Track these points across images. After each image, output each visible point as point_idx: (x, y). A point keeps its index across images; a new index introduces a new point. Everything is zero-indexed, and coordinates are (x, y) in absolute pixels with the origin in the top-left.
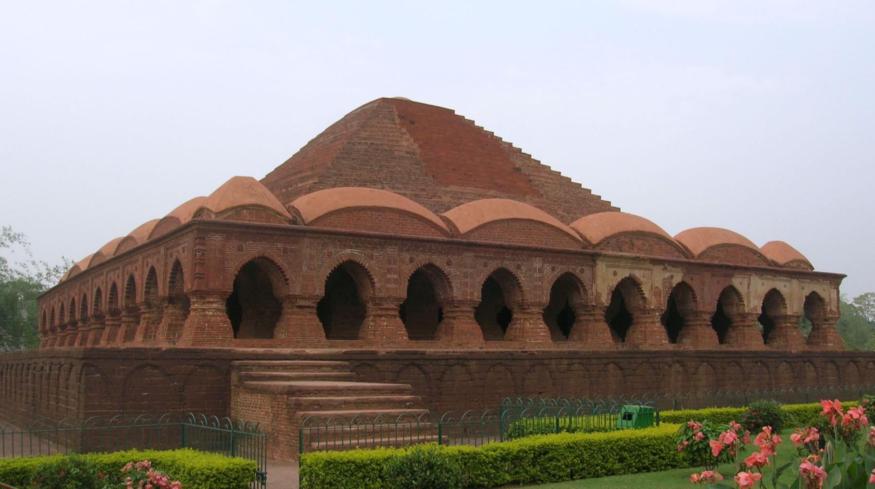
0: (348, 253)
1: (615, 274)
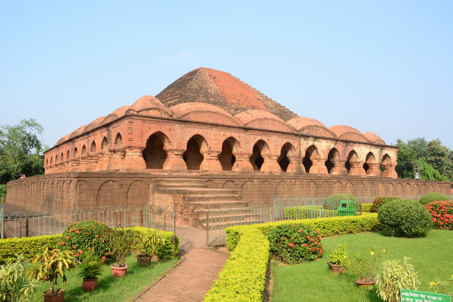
1: (307, 144)
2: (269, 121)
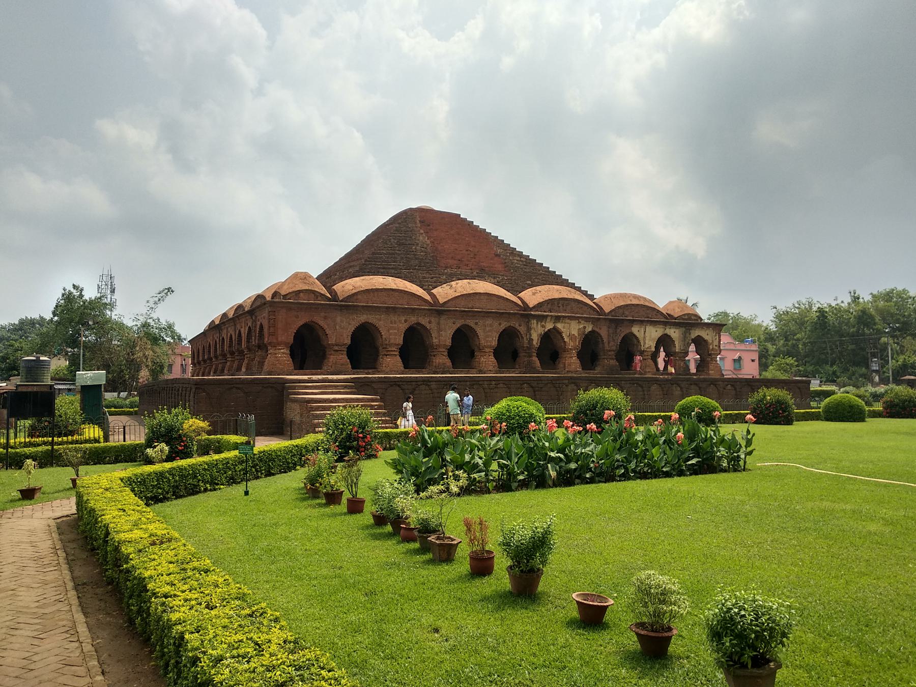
0: (363, 318)
1: (543, 326)
2: (482, 297)
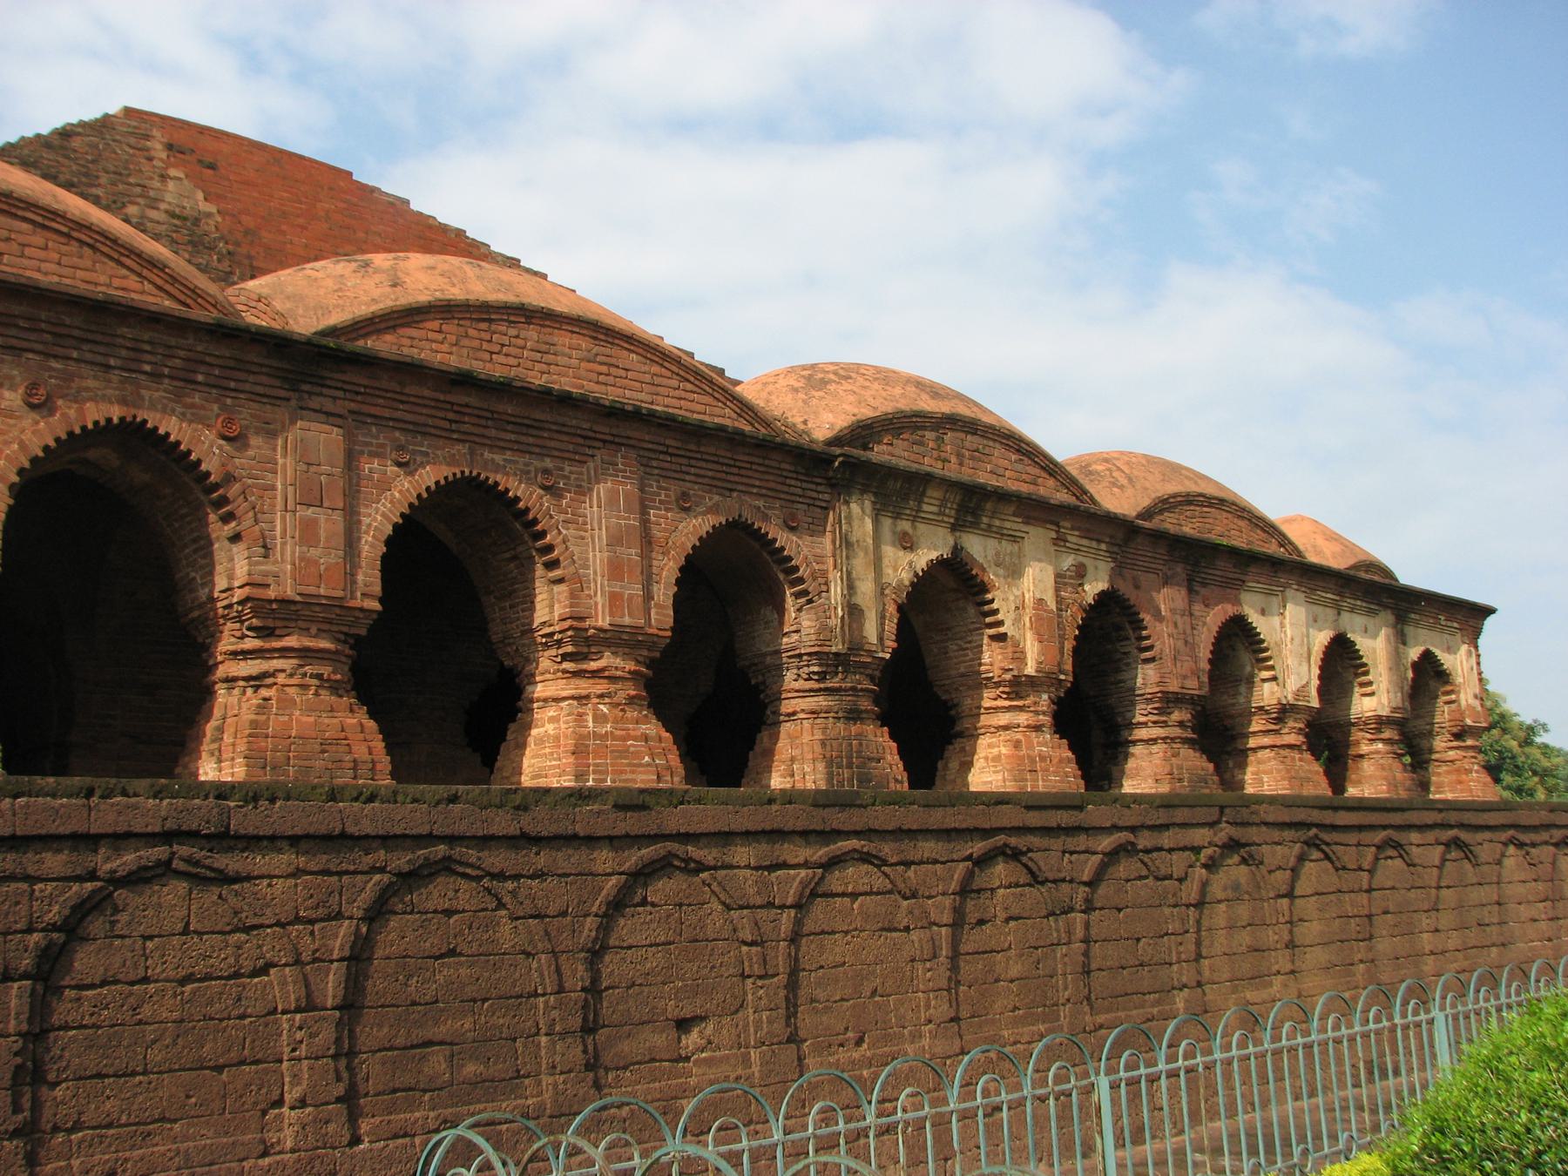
2: (563, 339)
